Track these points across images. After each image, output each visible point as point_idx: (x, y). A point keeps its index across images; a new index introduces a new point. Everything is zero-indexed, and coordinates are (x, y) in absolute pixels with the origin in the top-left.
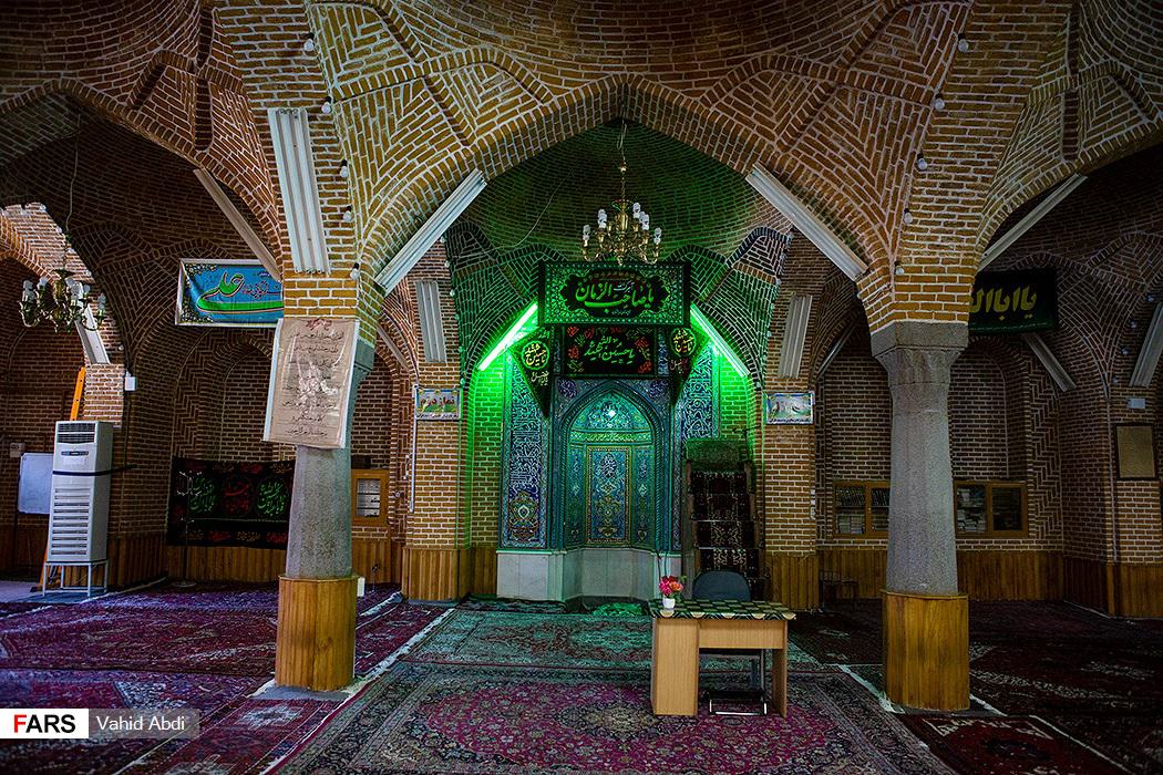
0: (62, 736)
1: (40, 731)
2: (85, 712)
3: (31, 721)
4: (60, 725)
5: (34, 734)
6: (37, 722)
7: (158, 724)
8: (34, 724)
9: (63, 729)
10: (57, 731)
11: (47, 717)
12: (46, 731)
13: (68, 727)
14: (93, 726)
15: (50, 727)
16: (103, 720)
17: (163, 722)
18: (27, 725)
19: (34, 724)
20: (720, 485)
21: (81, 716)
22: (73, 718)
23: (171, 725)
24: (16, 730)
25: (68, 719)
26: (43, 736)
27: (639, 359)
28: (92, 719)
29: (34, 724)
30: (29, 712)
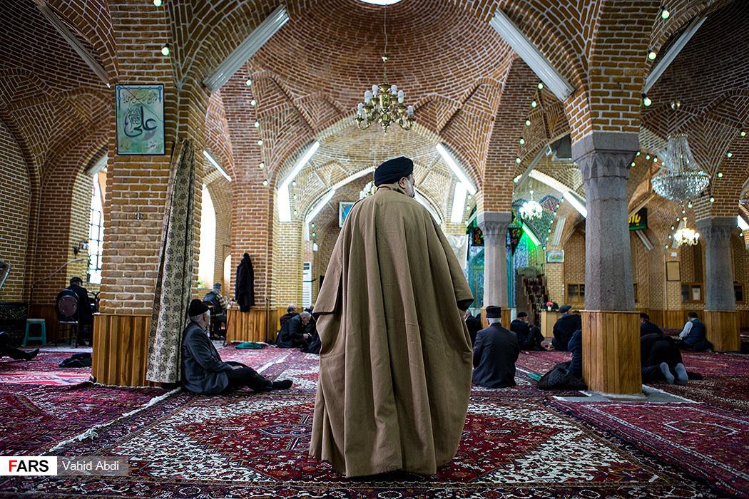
0: (40, 474)
1: (26, 471)
2: (55, 458)
3: (20, 465)
4: (39, 467)
5: (22, 473)
6: (24, 465)
7: (101, 466)
8: (22, 466)
9: (41, 469)
10: (37, 470)
11: (30, 462)
12: (30, 470)
13: (44, 468)
14: (60, 469)
15: (32, 468)
17: (105, 465)
18: (17, 467)
19: (22, 466)
20: (533, 283)
22: (47, 462)
23: (110, 467)
24: (10, 470)
25: (44, 463)
26: (28, 474)
29: (22, 466)
30: (19, 459)
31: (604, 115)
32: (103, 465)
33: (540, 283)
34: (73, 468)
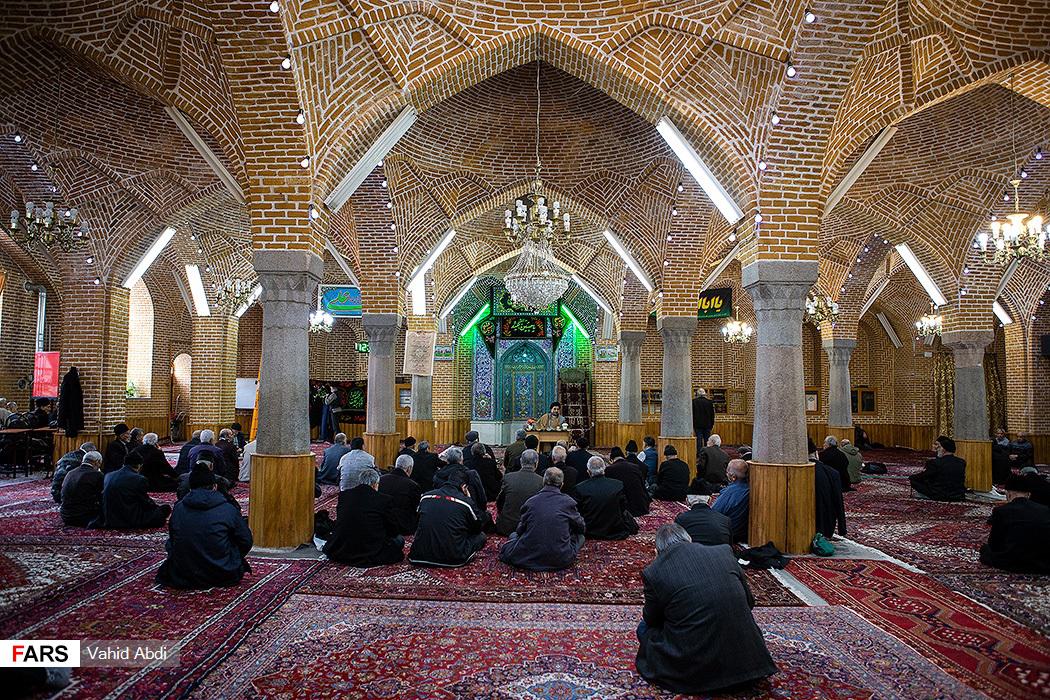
1: (36, 660)
2: (77, 643)
3: (28, 652)
4: (54, 655)
5: (31, 663)
6: (34, 652)
8: (30, 654)
9: (57, 658)
10: (52, 660)
11: (42, 647)
12: (42, 660)
13: (62, 657)
14: (83, 657)
15: (45, 657)
16: (93, 650)
18: (24, 655)
19: (31, 654)
20: (574, 390)
21: (73, 647)
22: (65, 649)
24: (15, 660)
25: (61, 650)
26: (39, 664)
27: (538, 330)
28: (83, 647)
29: (31, 654)
30: (27, 643)
31: (267, 230)
32: (145, 653)
33: (583, 390)
34: (103, 656)
